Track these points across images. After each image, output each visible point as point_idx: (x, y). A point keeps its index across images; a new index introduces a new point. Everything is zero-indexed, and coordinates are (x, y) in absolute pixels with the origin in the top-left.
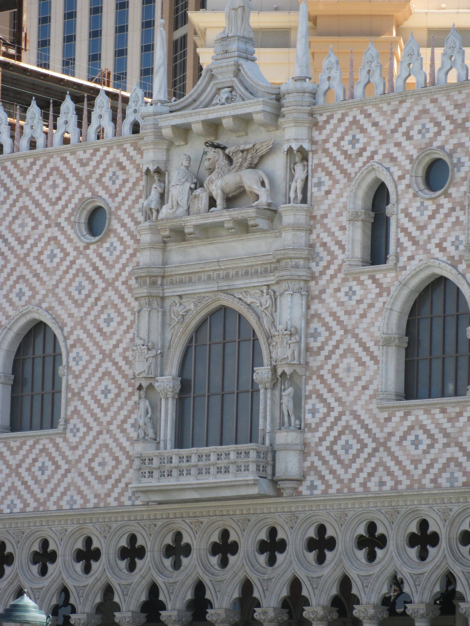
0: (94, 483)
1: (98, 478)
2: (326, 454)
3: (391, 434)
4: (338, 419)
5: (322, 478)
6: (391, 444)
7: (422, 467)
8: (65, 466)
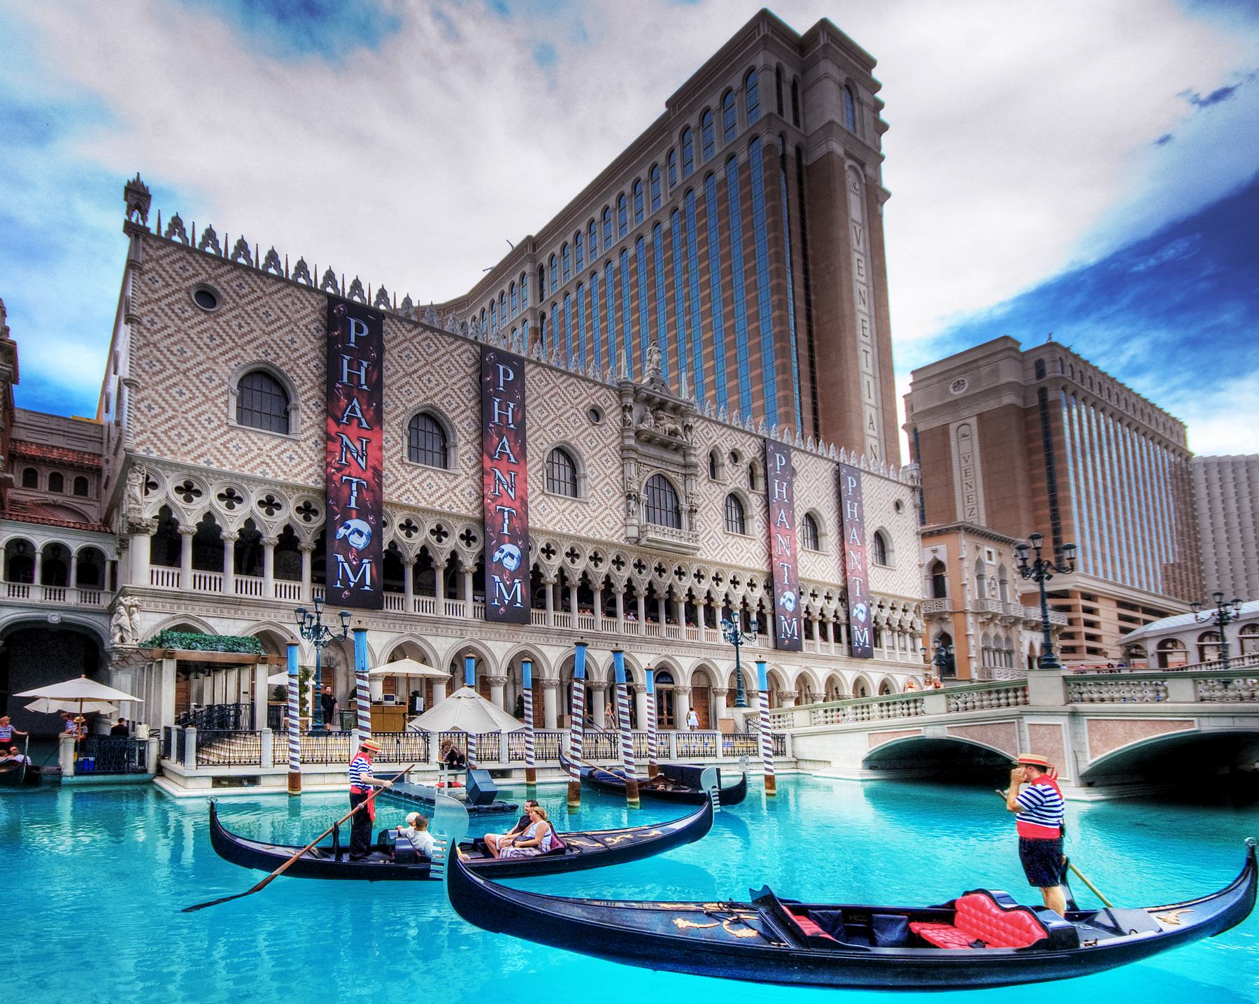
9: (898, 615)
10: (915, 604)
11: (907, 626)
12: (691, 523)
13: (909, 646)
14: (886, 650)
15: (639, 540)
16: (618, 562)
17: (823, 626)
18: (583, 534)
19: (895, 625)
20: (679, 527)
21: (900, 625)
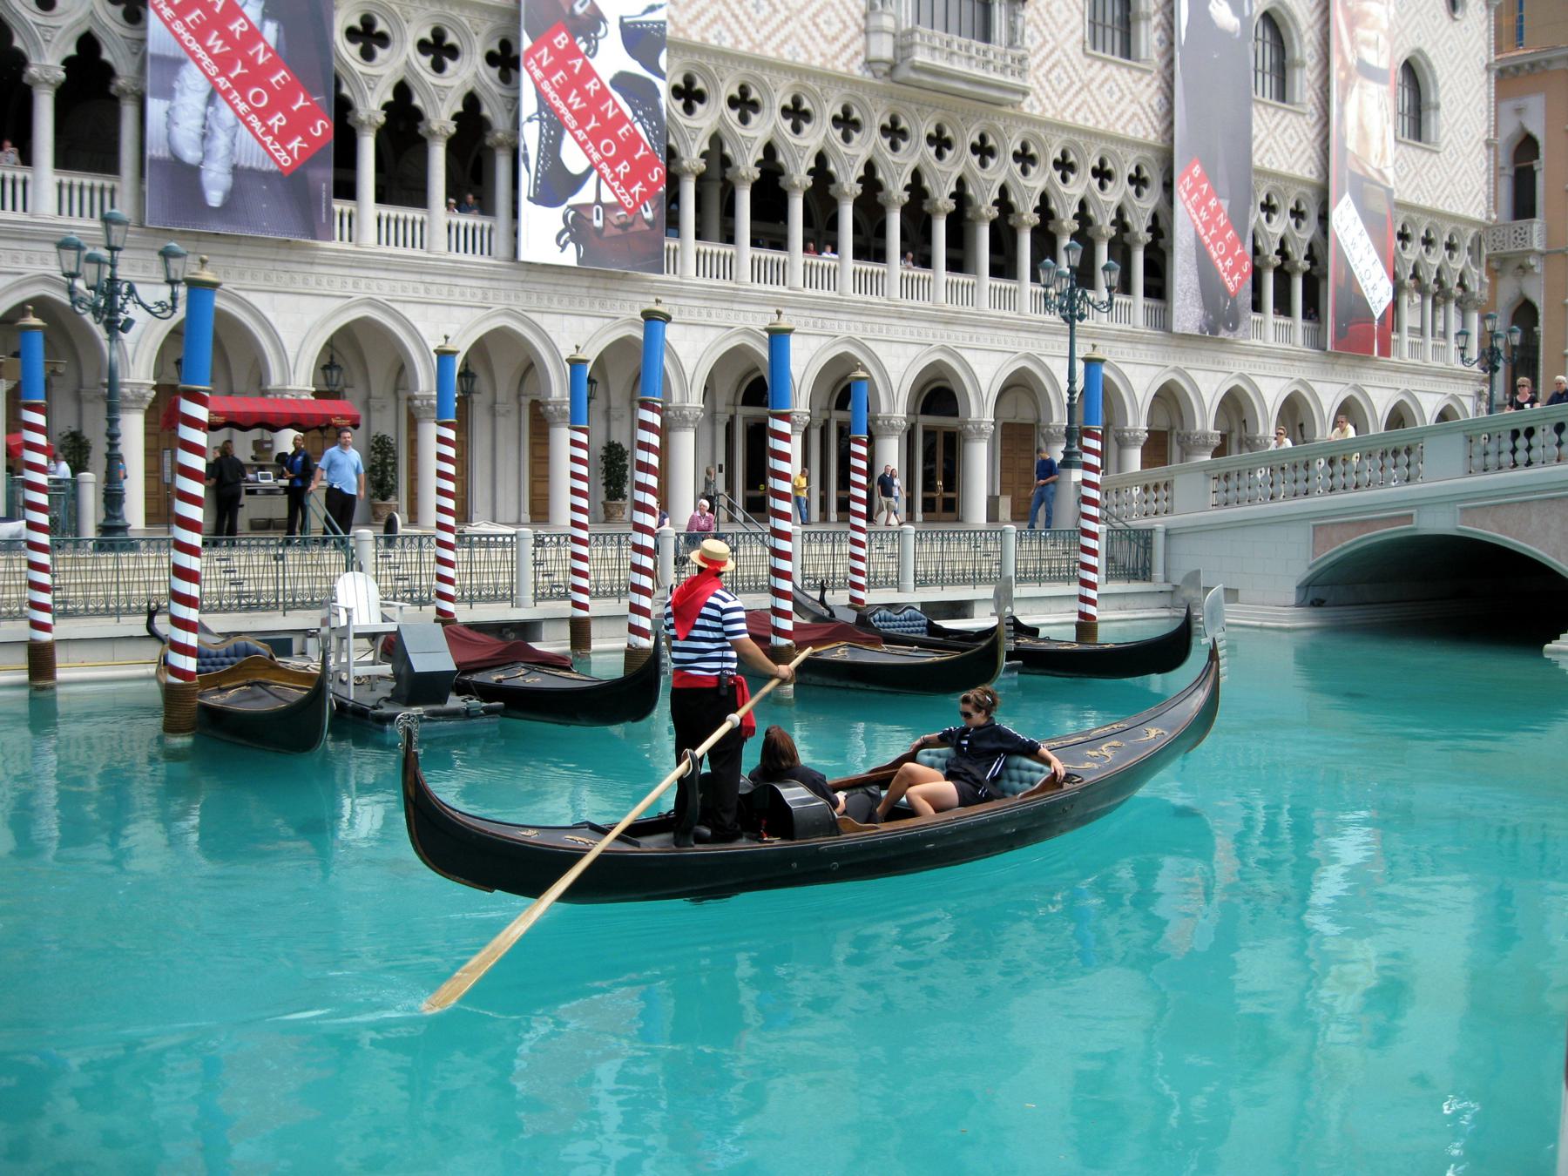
0: (820, 40)
1: (824, 36)
2: (1042, 79)
3: (1092, 80)
4: (1052, 52)
5: (1040, 100)
6: (1094, 86)
7: (1115, 114)
8: (783, 14)
9: (1437, 257)
10: (1472, 232)
11: (1452, 283)
12: (1012, 29)
13: (1455, 325)
14: (1406, 338)
15: (893, 67)
16: (846, 123)
17: (1283, 277)
18: (769, 52)
19: (1429, 279)
20: (986, 37)
21: (1415, 276)
